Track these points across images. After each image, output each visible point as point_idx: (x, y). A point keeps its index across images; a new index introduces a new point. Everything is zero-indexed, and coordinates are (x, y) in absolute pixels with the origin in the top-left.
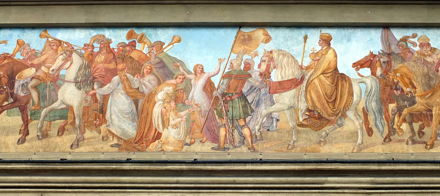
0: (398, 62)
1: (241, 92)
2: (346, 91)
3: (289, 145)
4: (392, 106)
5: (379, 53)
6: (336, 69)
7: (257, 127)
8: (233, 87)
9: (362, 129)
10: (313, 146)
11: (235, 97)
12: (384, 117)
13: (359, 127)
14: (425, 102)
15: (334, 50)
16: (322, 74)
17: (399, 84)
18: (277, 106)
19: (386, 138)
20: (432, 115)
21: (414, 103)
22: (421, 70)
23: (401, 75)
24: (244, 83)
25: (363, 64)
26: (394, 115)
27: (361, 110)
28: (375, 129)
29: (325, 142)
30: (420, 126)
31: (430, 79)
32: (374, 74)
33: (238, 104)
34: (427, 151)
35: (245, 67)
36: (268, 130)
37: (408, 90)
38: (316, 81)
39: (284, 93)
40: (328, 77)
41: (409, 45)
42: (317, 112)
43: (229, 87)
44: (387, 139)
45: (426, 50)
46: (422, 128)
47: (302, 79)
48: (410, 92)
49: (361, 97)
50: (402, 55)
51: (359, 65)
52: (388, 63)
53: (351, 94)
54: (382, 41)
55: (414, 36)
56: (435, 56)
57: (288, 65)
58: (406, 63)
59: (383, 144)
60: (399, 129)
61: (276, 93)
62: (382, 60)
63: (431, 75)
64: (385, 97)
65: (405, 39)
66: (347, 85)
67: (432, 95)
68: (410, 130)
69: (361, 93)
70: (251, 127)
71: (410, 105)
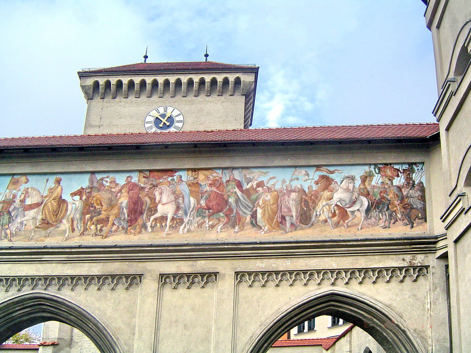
0: (96, 192)
1: (9, 210)
2: (64, 209)
3: (30, 238)
4: (88, 216)
5: (86, 187)
6: (61, 197)
7: (14, 229)
8: (5, 207)
9: (69, 228)
10: (42, 238)
11: (5, 213)
12: (82, 222)
13: (68, 228)
14: (107, 213)
15: (62, 187)
16: (53, 199)
17: (94, 204)
18: (26, 218)
19: (81, 233)
20: (108, 221)
21: (100, 213)
22: (108, 196)
23: (96, 199)
24: (11, 206)
25: (76, 194)
26: (88, 221)
27: (71, 219)
28: (76, 229)
29: (49, 236)
30: (101, 226)
31: (112, 201)
32: (81, 199)
33: (6, 217)
34: (102, 240)
35: (13, 197)
36: (20, 230)
37: (99, 207)
38: (49, 204)
39: (31, 211)
40: (56, 201)
41: (104, 182)
42: (47, 220)
43: (3, 208)
44: (82, 234)
45: (113, 185)
46: (102, 227)
47: (42, 203)
48: (99, 208)
49: (72, 211)
50: (99, 188)
51: (74, 194)
52: (90, 193)
53: (67, 210)
54: (89, 181)
55: (108, 177)
56: (117, 188)
57: (36, 195)
58: (100, 193)
59: (79, 236)
60: (90, 228)
61: (27, 210)
62: (87, 191)
63: (113, 199)
64: (85, 211)
65: (102, 179)
66: (65, 206)
67: (111, 209)
68: (95, 229)
69: (72, 209)
70: (11, 229)
71: (98, 216)
